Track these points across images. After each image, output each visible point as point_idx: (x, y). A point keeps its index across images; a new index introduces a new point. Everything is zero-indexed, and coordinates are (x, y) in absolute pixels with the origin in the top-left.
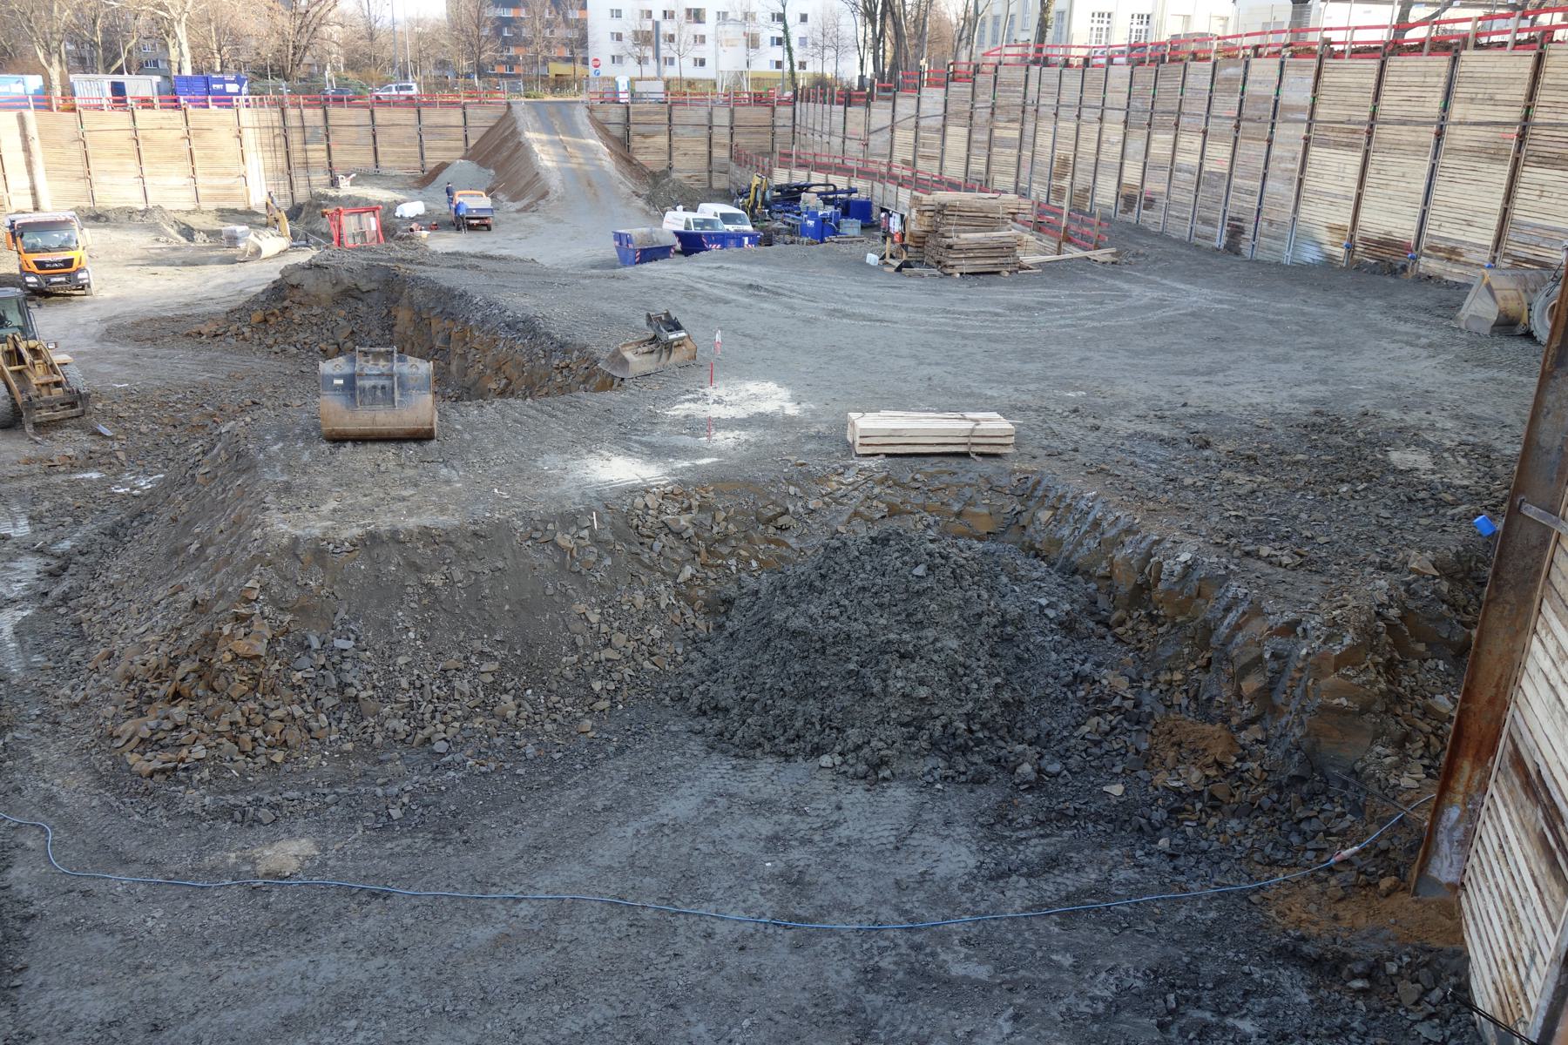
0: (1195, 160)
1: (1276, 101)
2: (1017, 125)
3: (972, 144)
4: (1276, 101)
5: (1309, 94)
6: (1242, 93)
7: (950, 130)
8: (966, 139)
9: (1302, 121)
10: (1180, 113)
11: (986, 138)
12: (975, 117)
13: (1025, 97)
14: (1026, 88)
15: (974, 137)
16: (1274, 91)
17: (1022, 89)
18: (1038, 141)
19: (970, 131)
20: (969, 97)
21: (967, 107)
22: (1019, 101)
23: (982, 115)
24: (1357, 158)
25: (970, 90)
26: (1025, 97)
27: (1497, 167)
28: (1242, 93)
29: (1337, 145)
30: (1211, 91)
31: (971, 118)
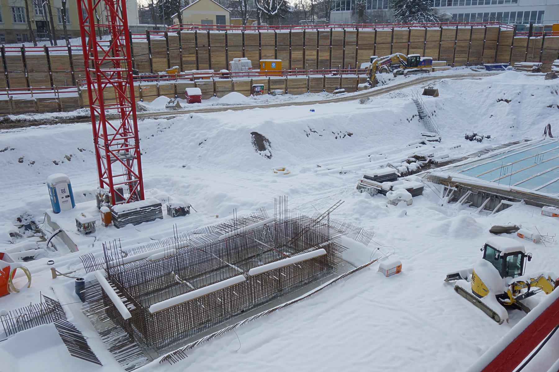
0: (316, 57)
1: (344, 41)
2: (194, 55)
4: (344, 41)
5: (355, 39)
6: (331, 39)
9: (355, 45)
14: (196, 40)
15: (171, 62)
16: (343, 39)
18: (212, 60)
19: (169, 60)
20: (166, 45)
26: (196, 44)
27: (405, 50)
28: (331, 39)
29: (366, 49)
30: (318, 39)
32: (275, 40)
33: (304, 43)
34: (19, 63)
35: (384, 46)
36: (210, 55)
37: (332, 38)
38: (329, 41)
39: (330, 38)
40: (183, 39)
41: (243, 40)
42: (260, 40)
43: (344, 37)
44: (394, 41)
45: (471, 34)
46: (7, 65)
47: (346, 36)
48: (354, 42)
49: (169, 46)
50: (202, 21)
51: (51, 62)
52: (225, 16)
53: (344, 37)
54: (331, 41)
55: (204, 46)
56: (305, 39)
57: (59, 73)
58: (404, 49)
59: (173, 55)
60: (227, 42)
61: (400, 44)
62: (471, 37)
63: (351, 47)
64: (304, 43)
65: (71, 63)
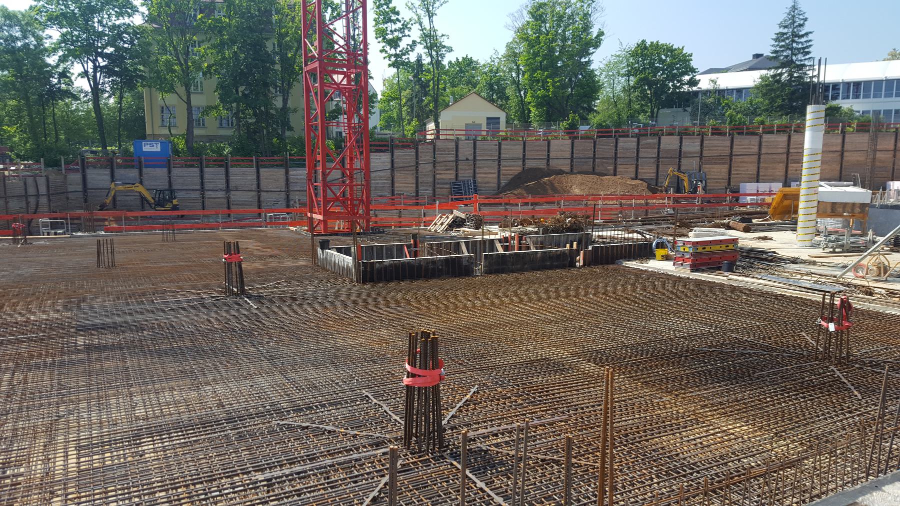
1: (680, 152)
2: (453, 172)
3: (420, 185)
4: (680, 152)
5: (699, 148)
6: (659, 148)
7: (397, 177)
8: (414, 182)
10: (616, 158)
11: (431, 179)
12: (420, 169)
13: (457, 156)
15: (420, 180)
17: (455, 152)
19: (417, 178)
20: (414, 158)
21: (413, 163)
22: (453, 159)
23: (426, 168)
24: (727, 167)
25: (414, 154)
26: (457, 156)
28: (659, 148)
29: (716, 163)
30: (638, 148)
31: (417, 171)
32: (569, 150)
33: (616, 154)
34: (219, 179)
35: (746, 158)
36: (474, 171)
37: (661, 147)
38: (656, 151)
39: (657, 147)
40: (439, 150)
41: (524, 151)
42: (549, 151)
43: (681, 146)
44: (763, 151)
45: (896, 142)
46: (205, 180)
47: (683, 143)
48: (697, 153)
49: (420, 159)
50: (466, 125)
51: (261, 177)
52: (499, 118)
53: (681, 146)
54: (659, 152)
55: (467, 159)
56: (618, 149)
57: (269, 193)
58: (779, 163)
59: (424, 171)
60: (500, 153)
61: (774, 156)
62: (896, 145)
63: (691, 160)
64: (616, 154)
65: (287, 180)
